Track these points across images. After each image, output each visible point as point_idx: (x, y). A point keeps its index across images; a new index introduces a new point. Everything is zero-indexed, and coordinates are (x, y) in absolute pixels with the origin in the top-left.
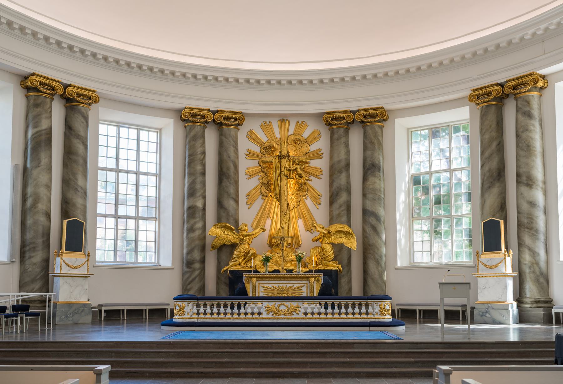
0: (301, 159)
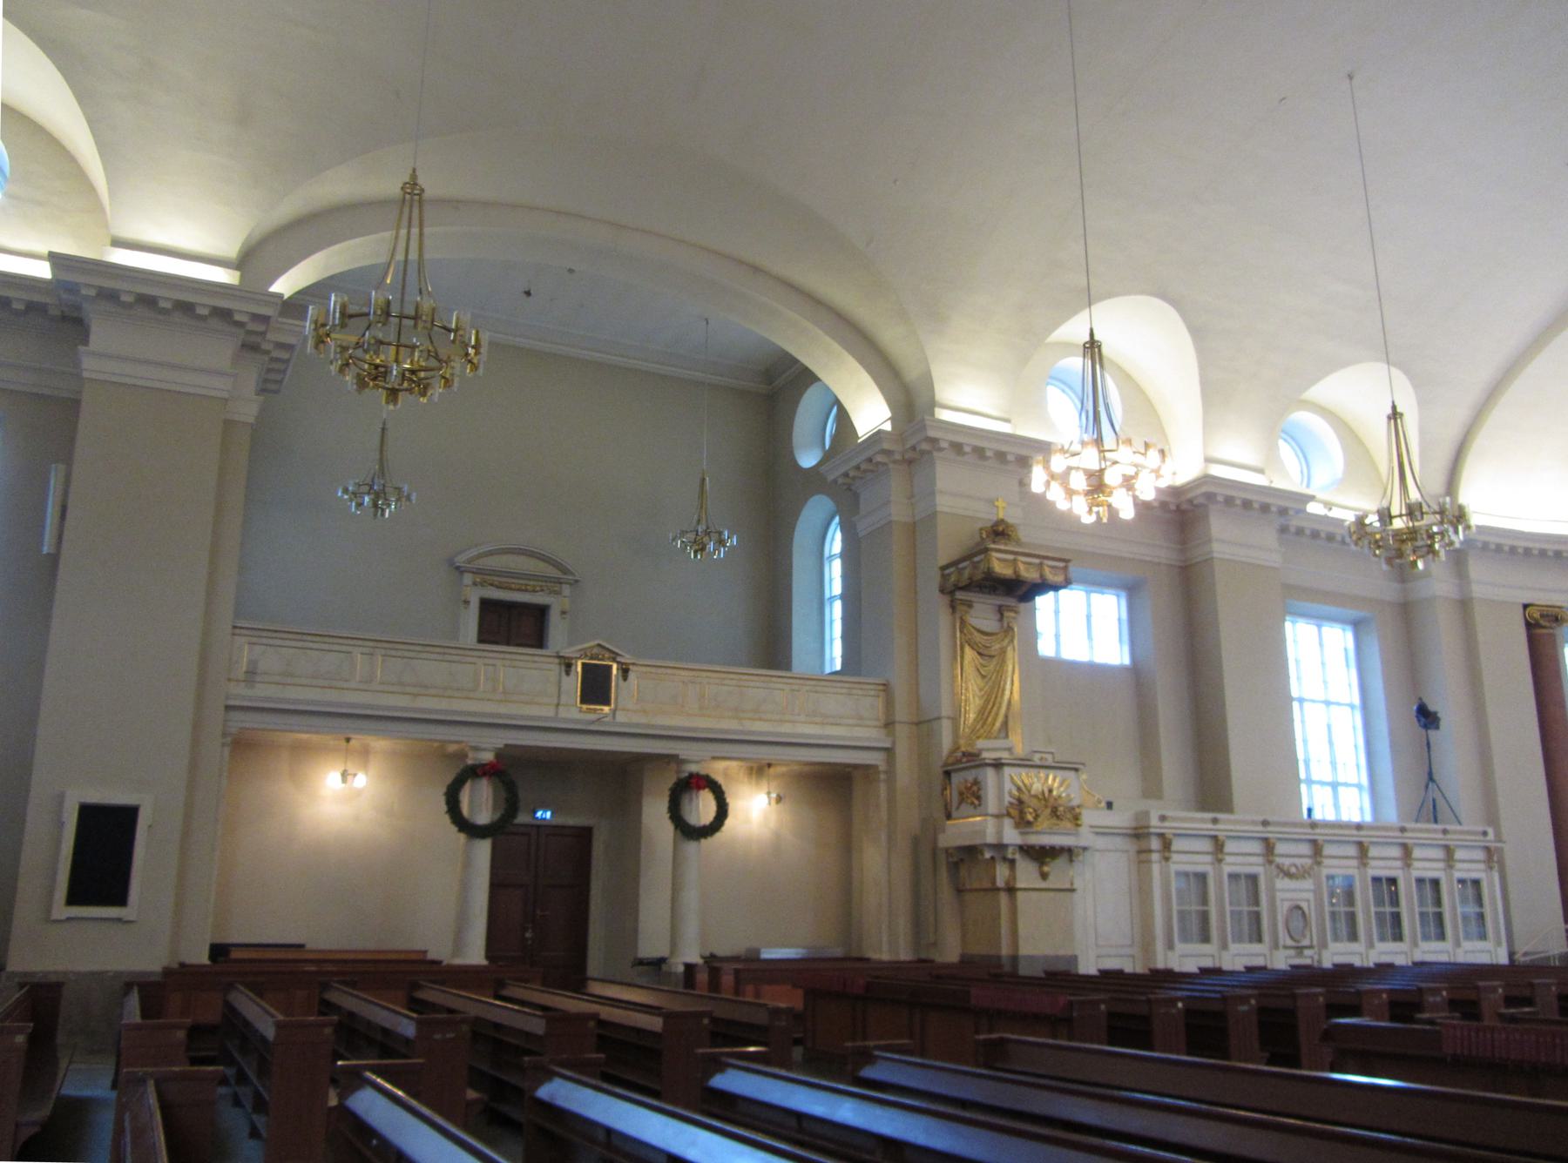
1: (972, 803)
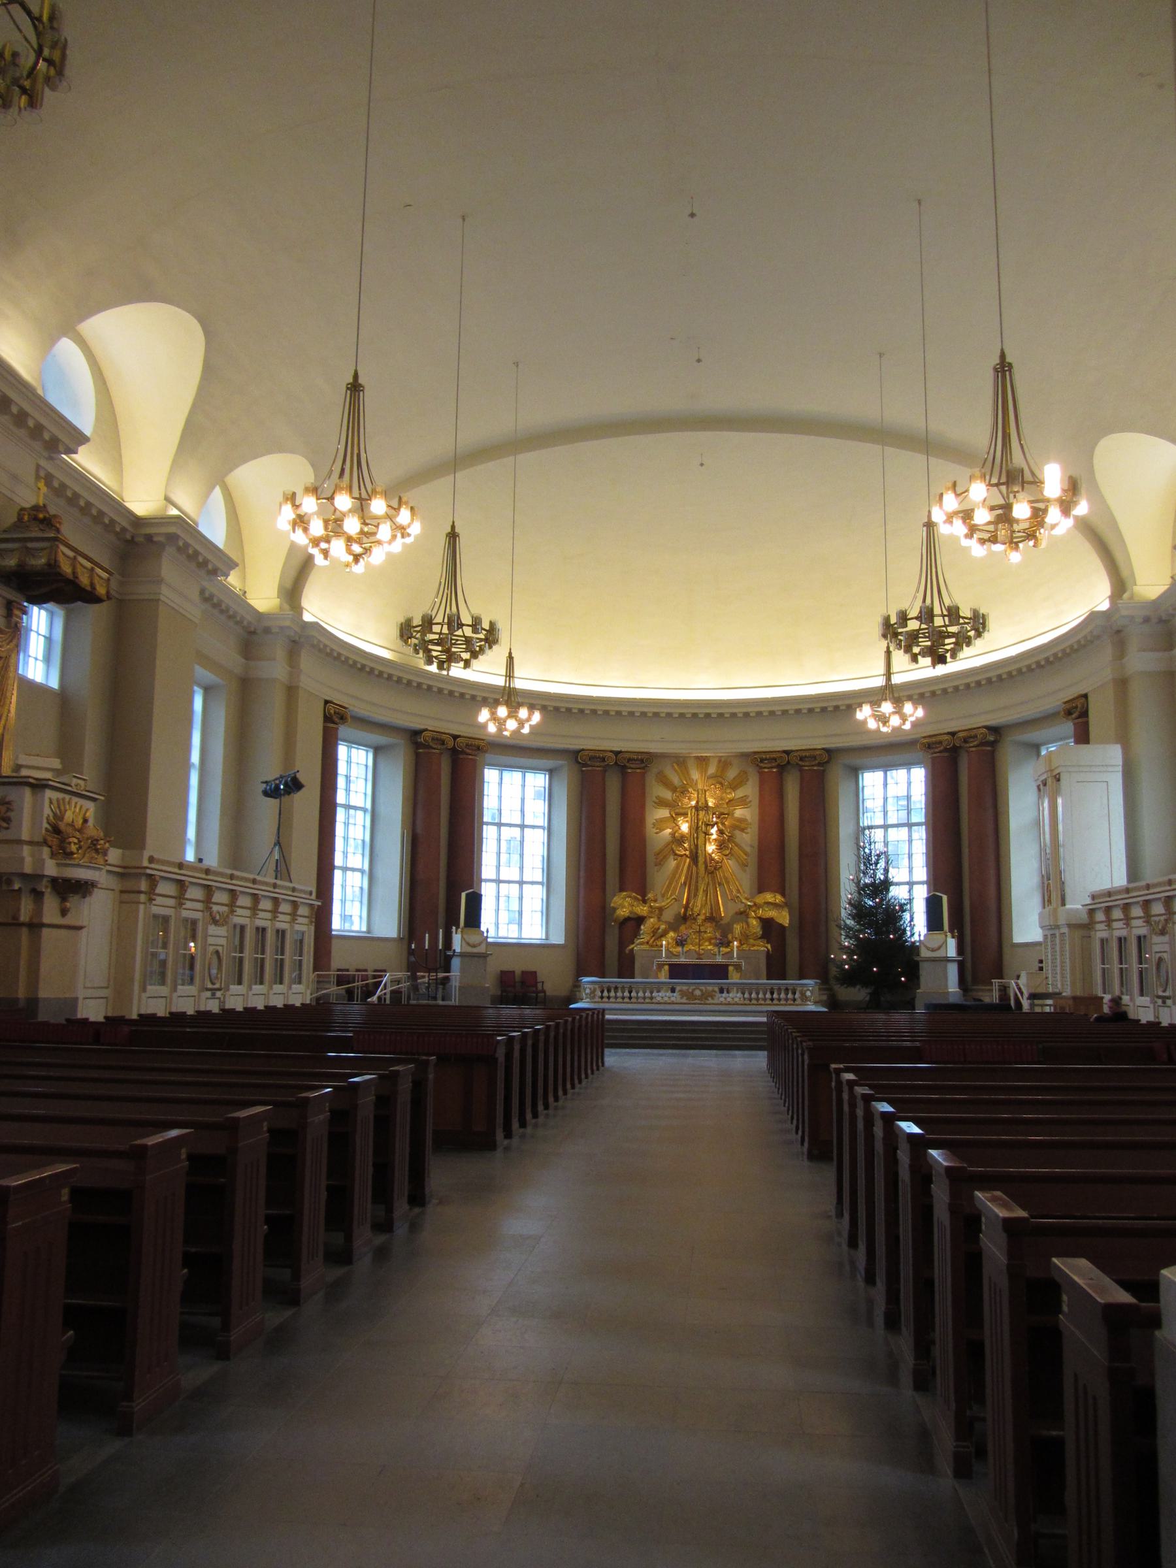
0: (722, 810)
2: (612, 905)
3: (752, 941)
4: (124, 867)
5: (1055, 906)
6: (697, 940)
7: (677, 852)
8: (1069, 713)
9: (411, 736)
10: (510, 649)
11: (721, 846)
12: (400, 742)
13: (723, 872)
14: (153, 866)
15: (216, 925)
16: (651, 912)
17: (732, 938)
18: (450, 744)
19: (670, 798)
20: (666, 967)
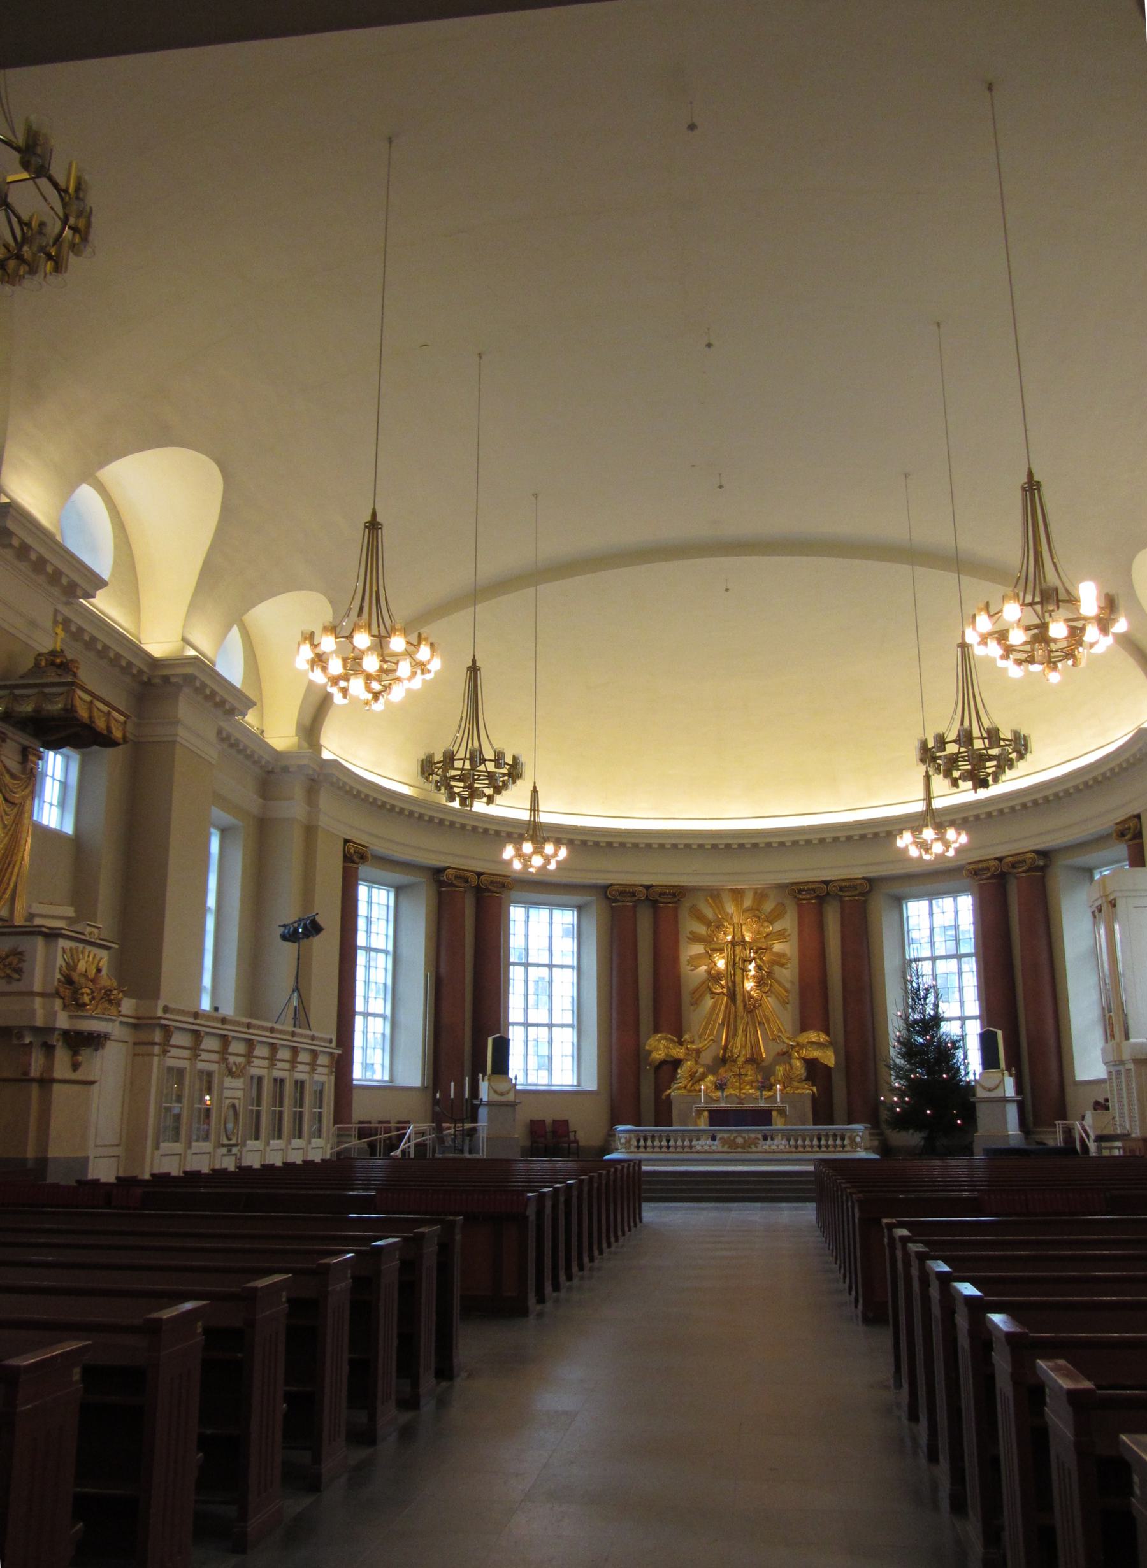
0: (760, 945)
1: (8, 977)
2: (647, 1048)
3: (795, 1084)
4: (138, 1018)
5: (1118, 1041)
6: (738, 1084)
7: (714, 990)
8: (1121, 835)
9: (434, 875)
10: (535, 783)
11: (760, 982)
12: (420, 879)
13: (763, 1011)
14: (167, 1016)
15: (232, 1077)
16: (687, 1054)
17: (775, 1080)
18: (474, 881)
19: (705, 933)
20: (706, 1114)
